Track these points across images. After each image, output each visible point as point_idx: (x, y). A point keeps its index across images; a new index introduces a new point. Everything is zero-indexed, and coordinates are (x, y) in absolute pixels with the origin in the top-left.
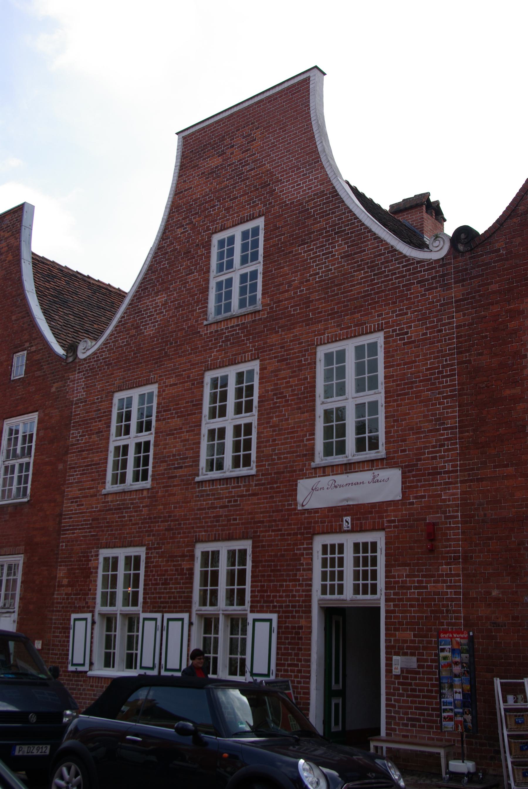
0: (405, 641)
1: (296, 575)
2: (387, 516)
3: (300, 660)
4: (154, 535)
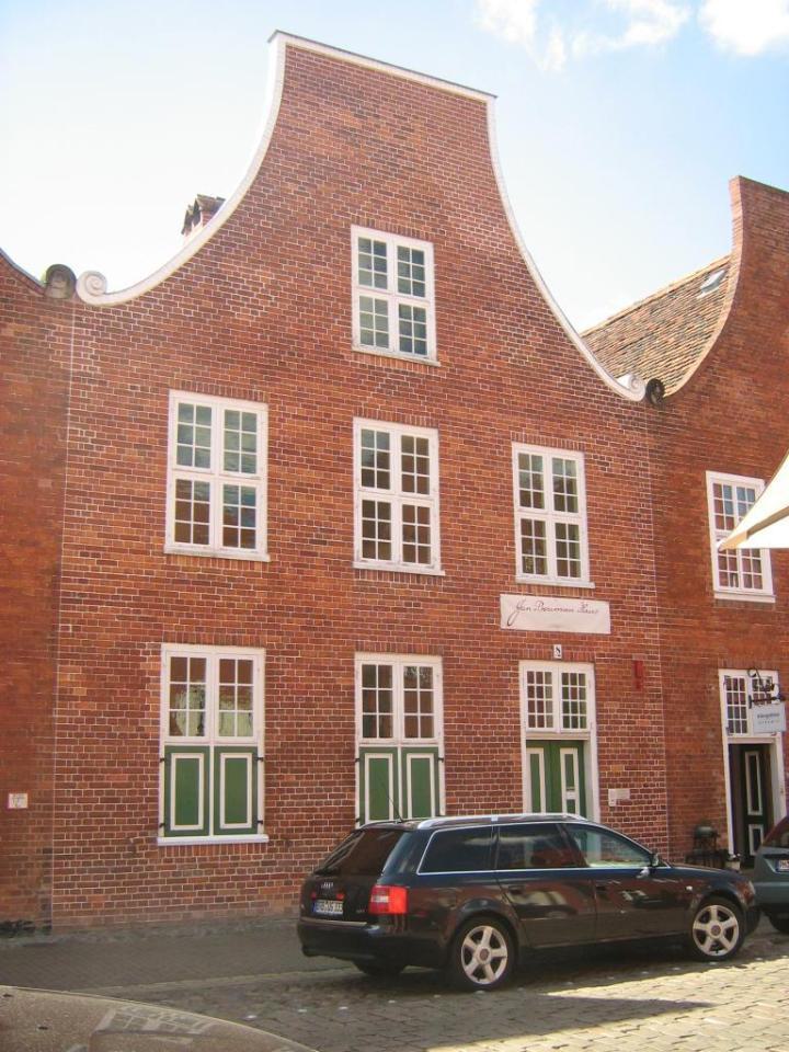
0: (618, 774)
1: (502, 704)
2: (597, 649)
3: (512, 799)
4: (280, 633)
